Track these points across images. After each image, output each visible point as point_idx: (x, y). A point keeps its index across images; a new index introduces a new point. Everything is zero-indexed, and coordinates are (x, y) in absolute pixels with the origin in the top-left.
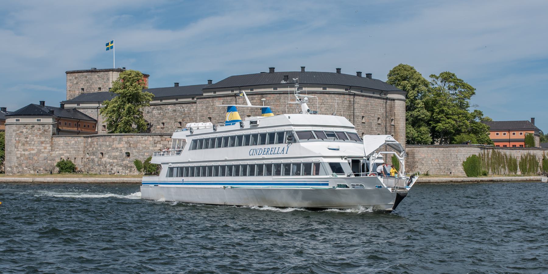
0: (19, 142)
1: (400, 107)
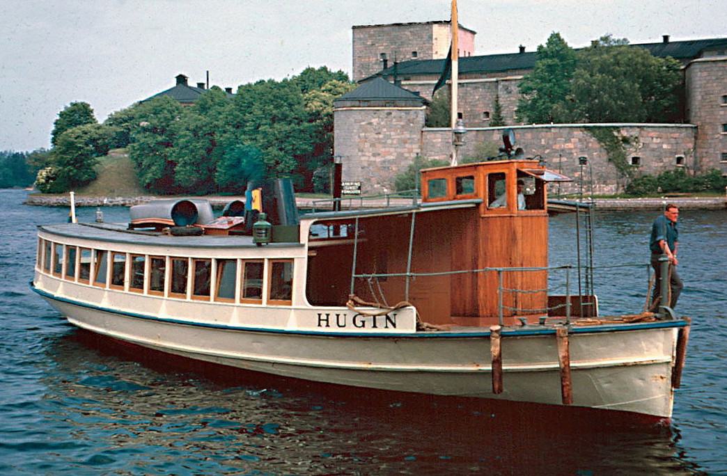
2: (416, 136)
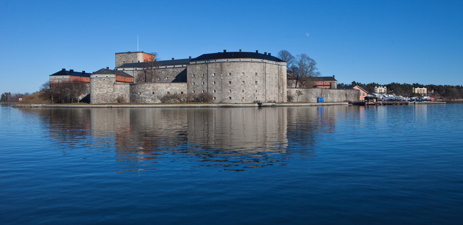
0: (97, 87)
1: (285, 69)
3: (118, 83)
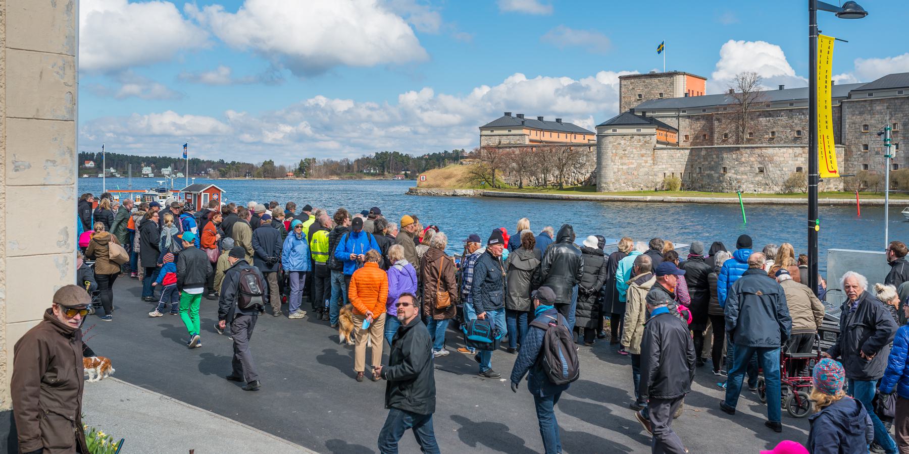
0: (616, 155)
2: (650, 152)
3: (658, 146)
